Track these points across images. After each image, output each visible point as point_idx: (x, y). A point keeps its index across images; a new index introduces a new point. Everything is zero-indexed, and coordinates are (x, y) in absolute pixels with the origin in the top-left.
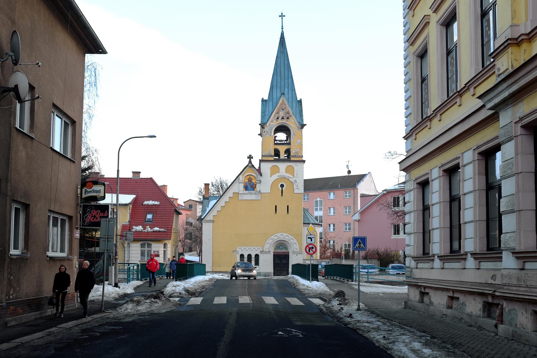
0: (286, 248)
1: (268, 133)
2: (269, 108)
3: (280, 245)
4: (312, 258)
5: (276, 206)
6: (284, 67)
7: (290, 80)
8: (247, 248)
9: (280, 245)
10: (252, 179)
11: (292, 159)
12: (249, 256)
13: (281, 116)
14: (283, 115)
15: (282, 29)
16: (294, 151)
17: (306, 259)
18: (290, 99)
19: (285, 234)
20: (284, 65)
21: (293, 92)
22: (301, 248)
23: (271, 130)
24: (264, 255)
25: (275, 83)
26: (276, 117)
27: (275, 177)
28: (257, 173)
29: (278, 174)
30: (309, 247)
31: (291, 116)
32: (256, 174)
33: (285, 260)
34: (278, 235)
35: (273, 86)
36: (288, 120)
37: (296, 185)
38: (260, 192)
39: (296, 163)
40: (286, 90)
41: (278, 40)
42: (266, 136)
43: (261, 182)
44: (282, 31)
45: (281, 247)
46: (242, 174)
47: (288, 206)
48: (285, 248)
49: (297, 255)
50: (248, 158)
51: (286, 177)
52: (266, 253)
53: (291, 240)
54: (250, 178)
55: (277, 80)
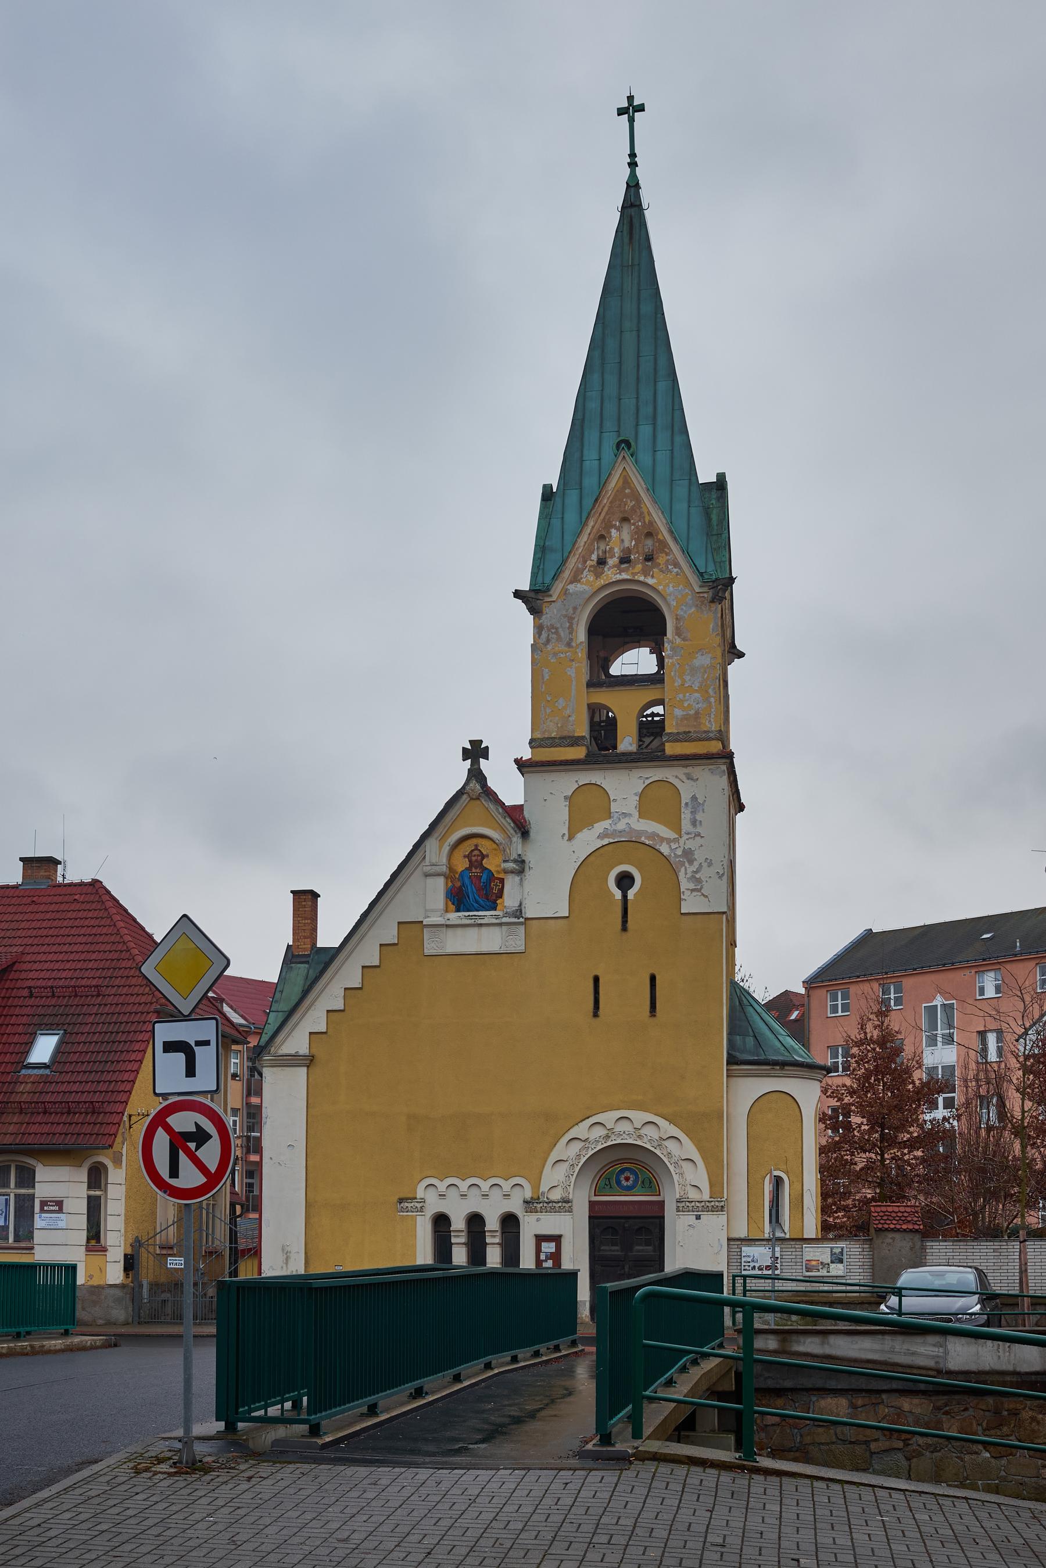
0: (651, 1184)
1: (557, 633)
2: (563, 518)
3: (622, 1171)
4: (779, 1234)
5: (596, 980)
6: (638, 331)
7: (663, 385)
8: (463, 1186)
9: (622, 1171)
10: (483, 856)
11: (670, 749)
12: (475, 1221)
13: (616, 550)
14: (627, 544)
15: (633, 165)
16: (678, 712)
17: (743, 1234)
18: (663, 470)
19: (639, 1117)
20: (639, 322)
21: (678, 439)
22: (716, 1184)
23: (571, 619)
24: (543, 1216)
25: (593, 405)
26: (594, 557)
27: (589, 840)
28: (508, 824)
29: (600, 827)
30: (168, 1129)
31: (663, 544)
32: (503, 830)
33: (648, 1243)
34: (609, 1117)
35: (583, 420)
36: (650, 564)
37: (689, 876)
38: (518, 912)
39: (689, 770)
40: (645, 430)
41: (614, 219)
42: (549, 647)
43: (527, 869)
44: (633, 175)
45: (627, 1179)
46: (436, 834)
47: (653, 979)
48: (643, 1182)
49: (698, 1218)
50: (466, 754)
51: (643, 839)
52: (553, 1210)
53: (671, 1145)
54: (476, 852)
55: (602, 390)
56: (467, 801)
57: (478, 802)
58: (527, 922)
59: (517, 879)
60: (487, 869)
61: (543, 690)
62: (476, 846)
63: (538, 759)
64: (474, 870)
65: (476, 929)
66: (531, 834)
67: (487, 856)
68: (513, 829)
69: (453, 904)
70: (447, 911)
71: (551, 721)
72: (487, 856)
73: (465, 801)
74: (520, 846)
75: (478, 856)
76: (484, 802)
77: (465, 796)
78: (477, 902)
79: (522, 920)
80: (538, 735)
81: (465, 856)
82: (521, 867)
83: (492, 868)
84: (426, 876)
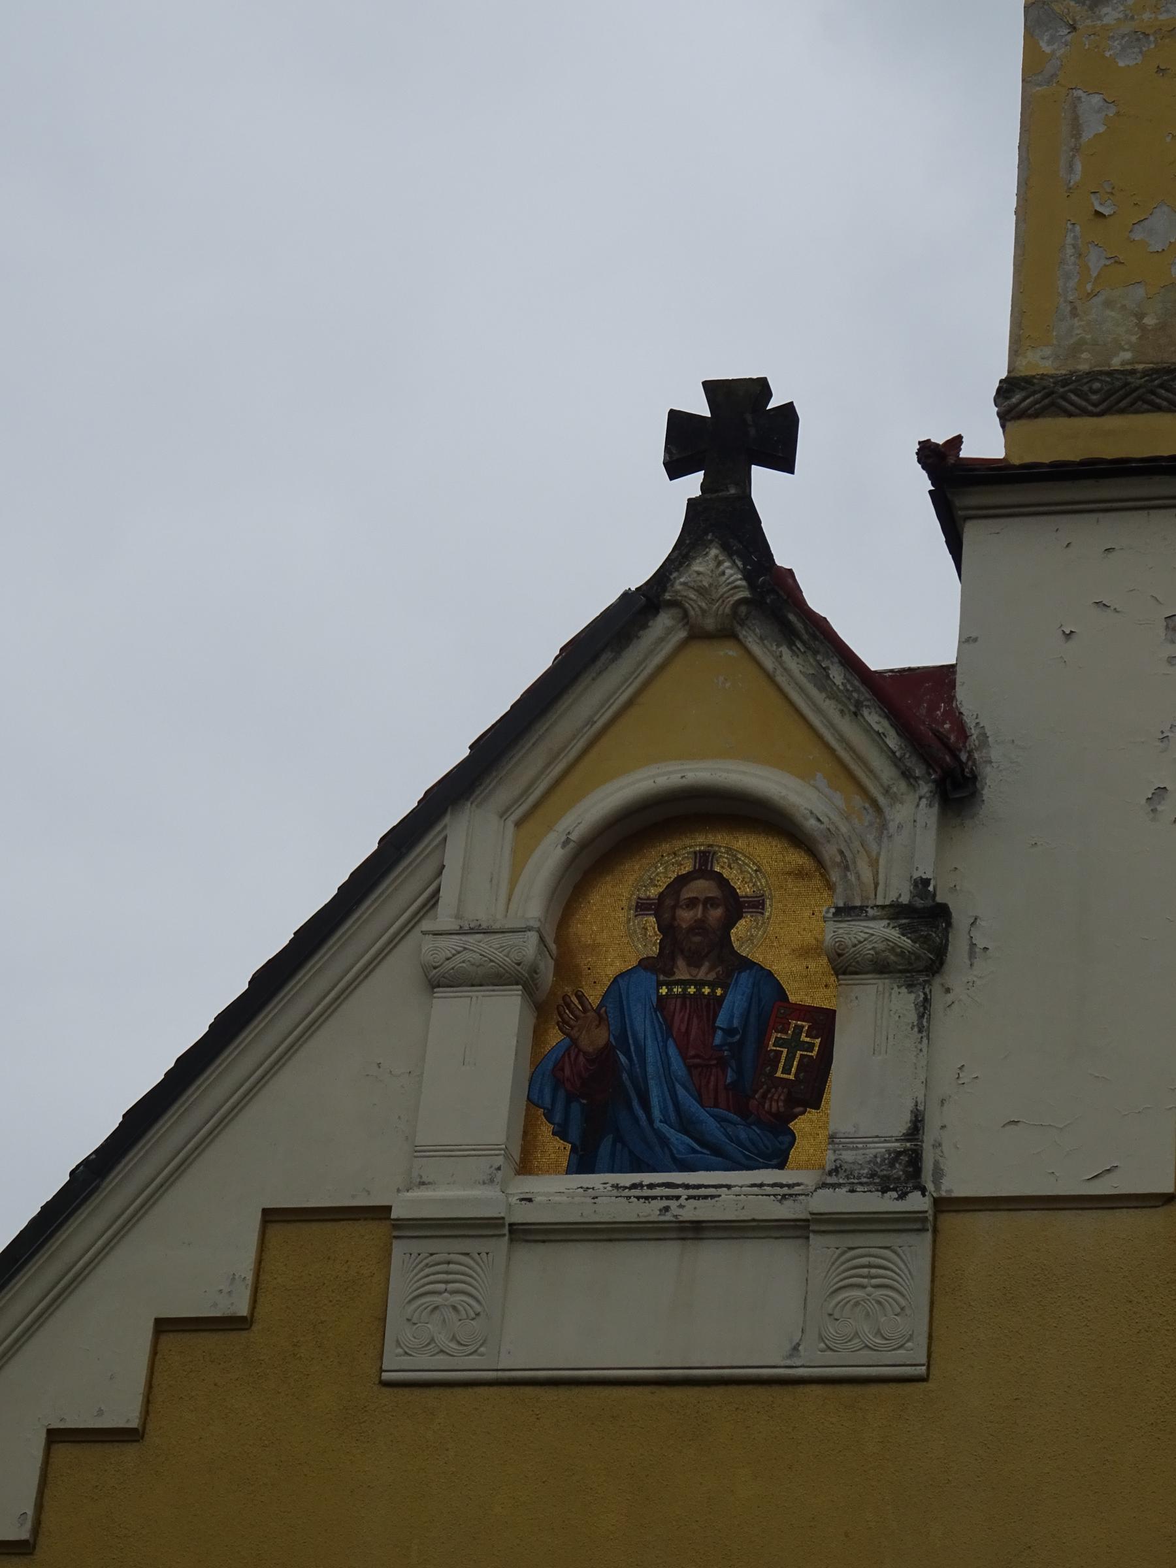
54: (701, 888)
56: (668, 648)
57: (729, 651)
58: (950, 1221)
59: (903, 1002)
60: (747, 964)
61: (1077, 177)
62: (704, 859)
63: (1045, 456)
64: (682, 972)
65: (666, 1256)
66: (988, 793)
67: (757, 904)
68: (895, 760)
69: (561, 1133)
70: (525, 1166)
71: (1108, 304)
72: (757, 904)
73: (662, 640)
74: (927, 840)
75: (709, 902)
76: (756, 650)
77: (664, 621)
78: (686, 1125)
79: (917, 1202)
80: (1042, 363)
81: (642, 907)
82: (925, 940)
83: (784, 967)
84: (434, 987)
